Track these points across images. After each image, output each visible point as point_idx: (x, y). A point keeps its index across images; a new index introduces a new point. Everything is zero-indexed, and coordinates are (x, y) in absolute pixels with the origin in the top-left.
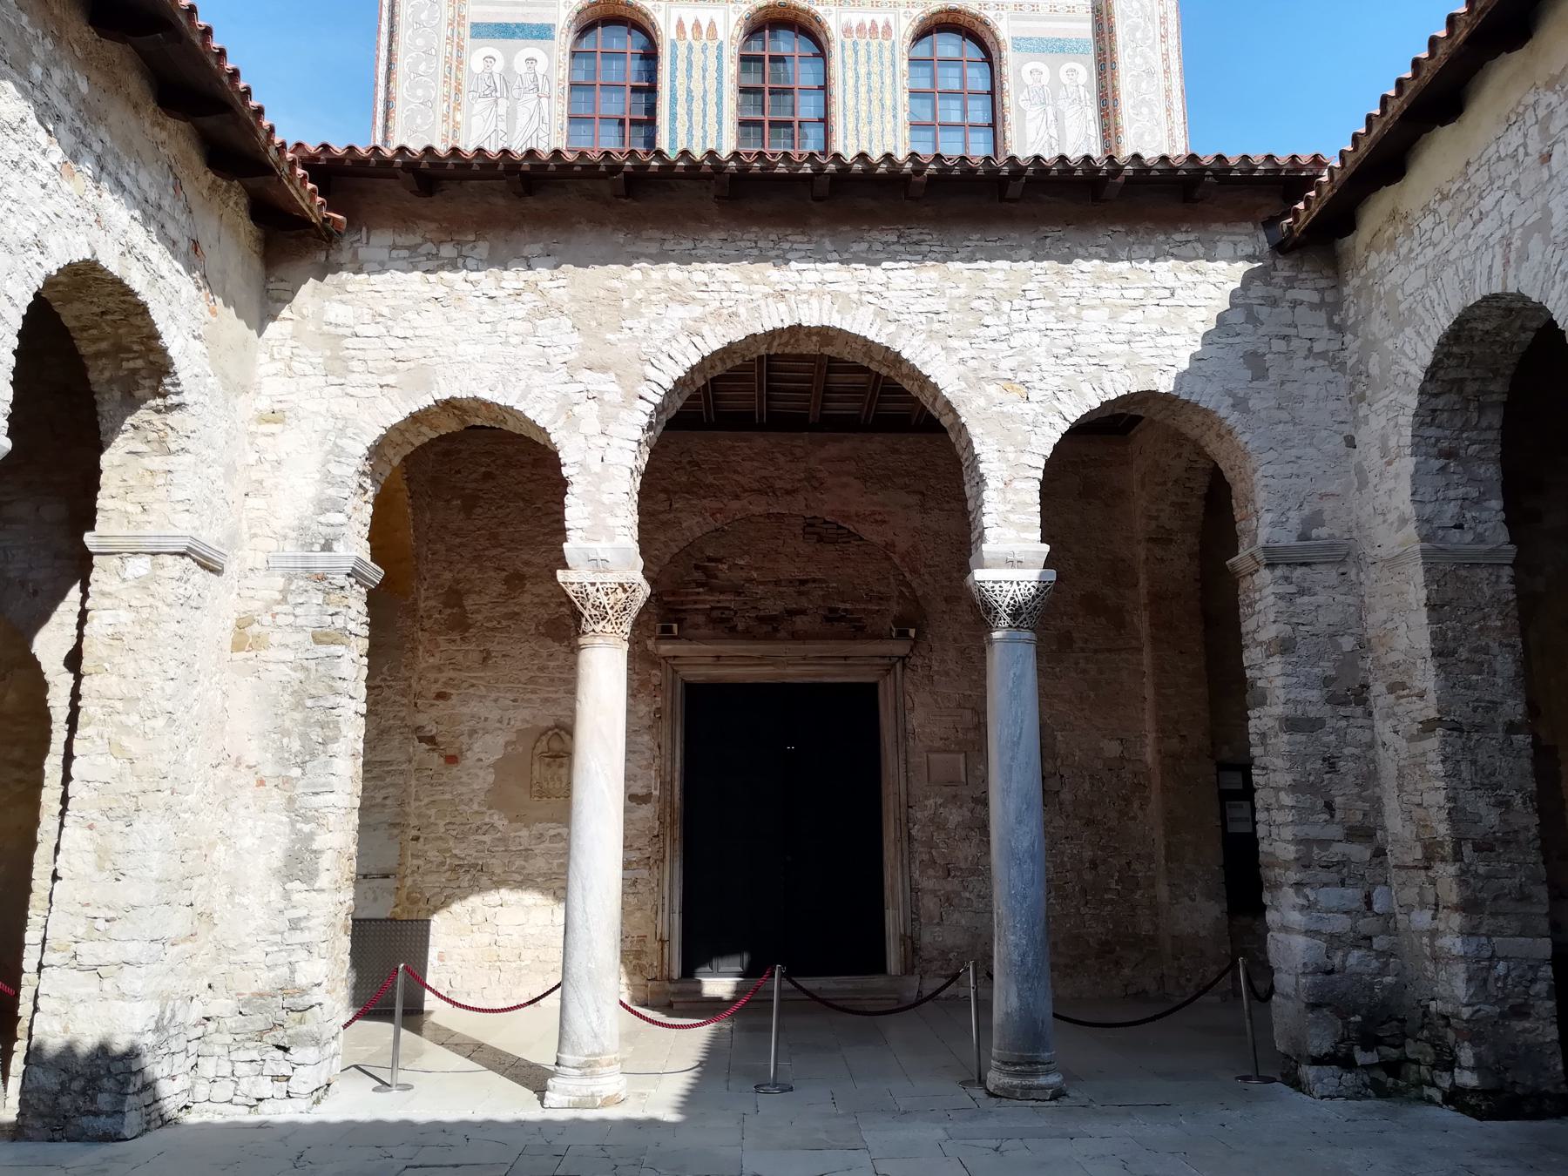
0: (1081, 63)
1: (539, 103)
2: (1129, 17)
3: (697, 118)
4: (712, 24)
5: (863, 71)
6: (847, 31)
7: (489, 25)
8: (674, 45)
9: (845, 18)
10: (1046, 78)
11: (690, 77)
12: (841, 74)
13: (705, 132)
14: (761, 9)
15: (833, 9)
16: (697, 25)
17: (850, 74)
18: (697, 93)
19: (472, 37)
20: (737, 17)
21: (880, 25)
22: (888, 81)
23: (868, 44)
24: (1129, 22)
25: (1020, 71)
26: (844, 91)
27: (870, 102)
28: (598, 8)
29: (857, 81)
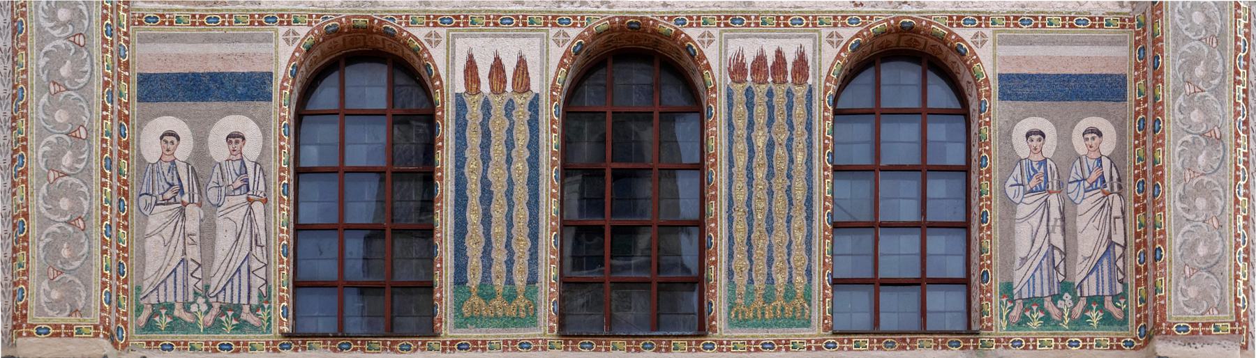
0: (1107, 116)
1: (250, 211)
2: (1186, 39)
3: (498, 229)
4: (522, 63)
5: (760, 142)
6: (737, 70)
7: (168, 77)
8: (461, 105)
9: (733, 47)
10: (1049, 147)
11: (486, 159)
12: (725, 142)
13: (511, 253)
14: (599, 34)
15: (715, 32)
16: (498, 67)
17: (741, 146)
18: (499, 189)
19: (140, 100)
20: (562, 51)
21: (790, 58)
22: (800, 158)
23: (770, 94)
24: (1185, 48)
25: (1009, 134)
26: (730, 176)
27: (771, 193)
28: (339, 39)
29: (751, 159)
